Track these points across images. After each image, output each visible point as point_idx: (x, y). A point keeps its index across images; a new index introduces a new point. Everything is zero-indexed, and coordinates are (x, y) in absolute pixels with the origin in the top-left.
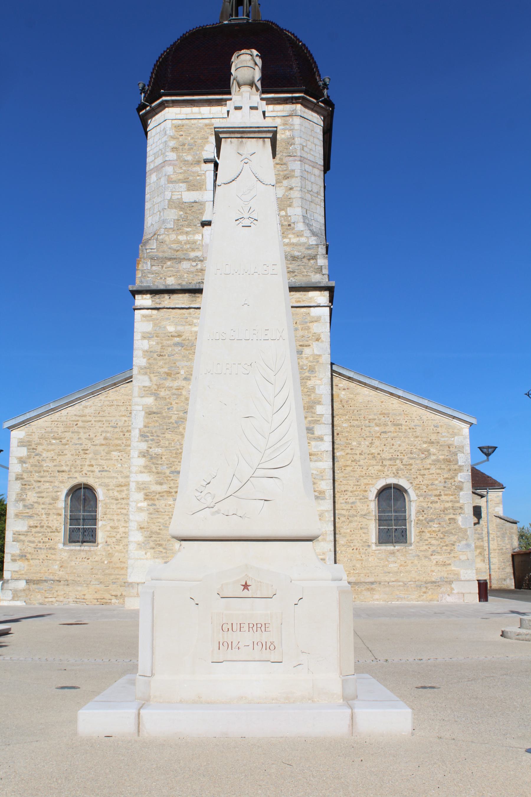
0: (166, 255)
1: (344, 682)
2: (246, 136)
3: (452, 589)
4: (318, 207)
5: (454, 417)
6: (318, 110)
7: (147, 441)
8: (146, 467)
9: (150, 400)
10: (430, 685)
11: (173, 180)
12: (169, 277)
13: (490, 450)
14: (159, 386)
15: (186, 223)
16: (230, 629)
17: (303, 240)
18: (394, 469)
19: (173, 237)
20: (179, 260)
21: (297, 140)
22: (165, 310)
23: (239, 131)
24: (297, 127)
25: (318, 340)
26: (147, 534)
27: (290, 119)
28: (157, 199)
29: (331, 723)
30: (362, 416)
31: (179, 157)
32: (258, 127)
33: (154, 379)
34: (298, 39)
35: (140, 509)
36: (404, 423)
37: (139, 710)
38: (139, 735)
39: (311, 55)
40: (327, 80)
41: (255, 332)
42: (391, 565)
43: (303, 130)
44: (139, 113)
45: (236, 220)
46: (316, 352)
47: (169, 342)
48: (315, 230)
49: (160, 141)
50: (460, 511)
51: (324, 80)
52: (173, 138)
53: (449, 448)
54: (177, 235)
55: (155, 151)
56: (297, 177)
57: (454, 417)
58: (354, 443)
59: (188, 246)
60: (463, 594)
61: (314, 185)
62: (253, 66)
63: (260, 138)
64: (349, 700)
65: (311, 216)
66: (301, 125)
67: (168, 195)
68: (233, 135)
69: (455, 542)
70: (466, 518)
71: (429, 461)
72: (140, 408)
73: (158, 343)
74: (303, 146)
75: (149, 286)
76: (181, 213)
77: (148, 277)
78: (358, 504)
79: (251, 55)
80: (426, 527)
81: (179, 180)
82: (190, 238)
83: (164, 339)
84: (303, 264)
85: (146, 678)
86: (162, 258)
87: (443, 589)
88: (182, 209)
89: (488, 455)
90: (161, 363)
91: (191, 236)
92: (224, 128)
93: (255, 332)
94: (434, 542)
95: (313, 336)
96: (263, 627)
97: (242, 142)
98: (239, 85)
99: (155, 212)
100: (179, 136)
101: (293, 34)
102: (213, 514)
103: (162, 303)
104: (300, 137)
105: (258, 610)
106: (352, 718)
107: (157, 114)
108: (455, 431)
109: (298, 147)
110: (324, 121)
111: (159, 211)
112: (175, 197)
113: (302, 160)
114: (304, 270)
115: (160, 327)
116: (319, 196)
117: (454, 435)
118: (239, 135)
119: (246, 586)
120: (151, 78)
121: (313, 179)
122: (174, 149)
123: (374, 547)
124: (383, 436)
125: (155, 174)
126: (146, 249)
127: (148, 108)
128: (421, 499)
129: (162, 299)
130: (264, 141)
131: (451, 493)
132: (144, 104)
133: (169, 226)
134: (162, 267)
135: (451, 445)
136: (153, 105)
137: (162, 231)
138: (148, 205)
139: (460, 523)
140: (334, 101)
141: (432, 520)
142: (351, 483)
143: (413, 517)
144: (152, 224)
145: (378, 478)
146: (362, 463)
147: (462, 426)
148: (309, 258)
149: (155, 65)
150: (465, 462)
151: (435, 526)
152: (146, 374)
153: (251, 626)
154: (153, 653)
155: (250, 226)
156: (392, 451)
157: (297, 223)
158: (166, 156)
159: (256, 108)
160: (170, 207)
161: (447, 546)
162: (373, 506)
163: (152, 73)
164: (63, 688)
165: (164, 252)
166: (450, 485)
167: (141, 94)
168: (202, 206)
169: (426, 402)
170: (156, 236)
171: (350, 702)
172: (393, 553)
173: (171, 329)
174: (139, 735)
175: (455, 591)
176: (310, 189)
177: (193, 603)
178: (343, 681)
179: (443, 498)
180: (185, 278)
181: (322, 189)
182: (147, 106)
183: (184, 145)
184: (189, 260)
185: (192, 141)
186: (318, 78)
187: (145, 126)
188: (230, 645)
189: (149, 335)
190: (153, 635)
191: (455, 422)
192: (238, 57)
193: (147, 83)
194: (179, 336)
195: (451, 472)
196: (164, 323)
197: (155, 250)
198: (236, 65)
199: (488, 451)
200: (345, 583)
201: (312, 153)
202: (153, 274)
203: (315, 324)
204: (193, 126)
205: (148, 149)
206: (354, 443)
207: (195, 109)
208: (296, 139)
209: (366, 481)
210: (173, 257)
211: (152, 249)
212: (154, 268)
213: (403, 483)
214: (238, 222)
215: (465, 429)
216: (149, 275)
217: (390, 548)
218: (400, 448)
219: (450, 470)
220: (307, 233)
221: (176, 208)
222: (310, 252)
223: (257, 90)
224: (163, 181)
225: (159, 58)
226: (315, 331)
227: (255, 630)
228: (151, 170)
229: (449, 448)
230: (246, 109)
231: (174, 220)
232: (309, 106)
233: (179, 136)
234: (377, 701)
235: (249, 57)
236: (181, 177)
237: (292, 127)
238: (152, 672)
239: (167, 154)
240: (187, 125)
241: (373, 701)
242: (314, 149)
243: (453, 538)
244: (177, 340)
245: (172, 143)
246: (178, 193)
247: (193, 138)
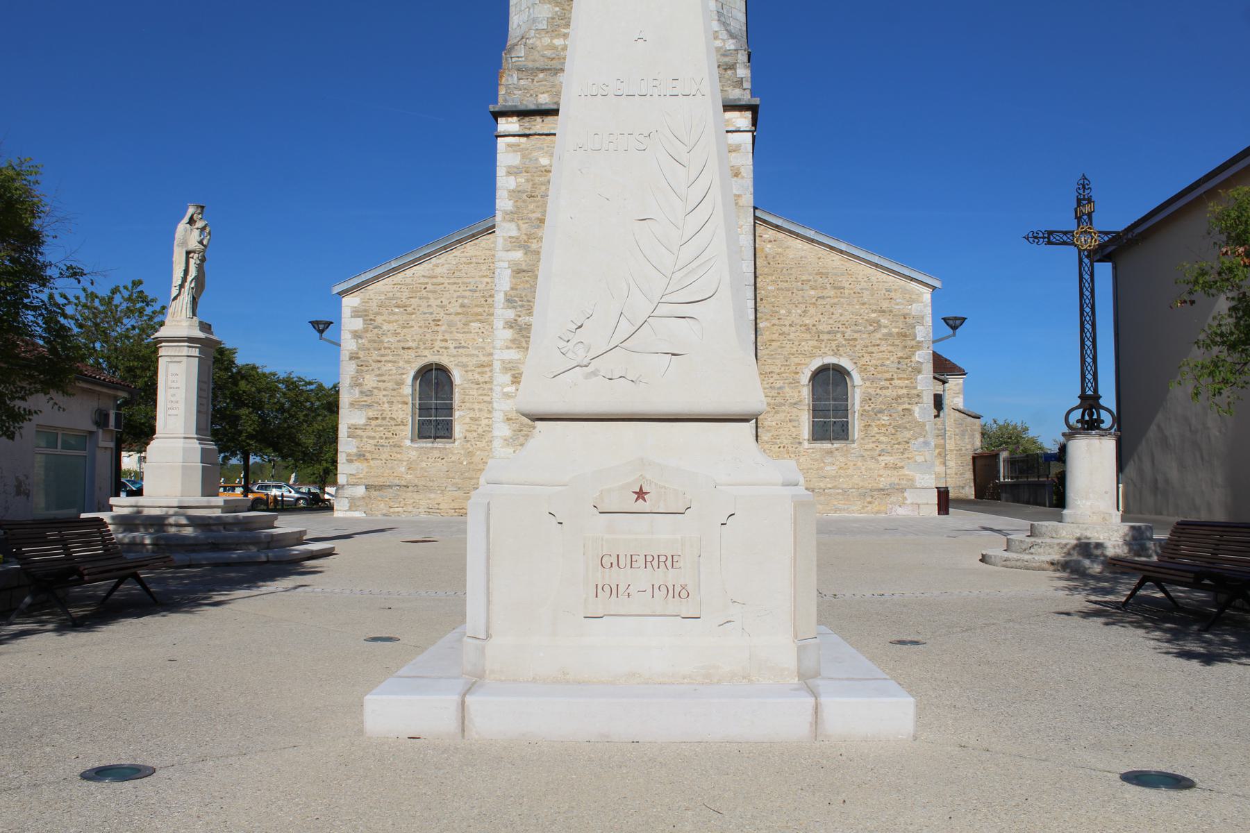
0: (537, 65)
1: (801, 649)
3: (905, 499)
5: (912, 279)
7: (514, 307)
8: (513, 341)
9: (518, 255)
10: (909, 638)
13: (958, 322)
14: (530, 236)
17: (718, 43)
18: (834, 344)
19: (546, 41)
25: (736, 175)
26: (516, 427)
29: (781, 719)
30: (793, 278)
33: (524, 227)
35: (507, 396)
36: (847, 285)
37: (464, 695)
38: (463, 737)
41: (655, 83)
42: (828, 468)
46: (735, 192)
50: (917, 400)
54: (552, 38)
58: (783, 312)
60: (919, 505)
64: (808, 680)
71: (878, 335)
72: (506, 264)
73: (527, 181)
78: (787, 389)
80: (873, 420)
87: (893, 499)
89: (954, 328)
90: (532, 207)
93: (655, 83)
94: (883, 439)
96: (669, 561)
102: (588, 376)
105: (660, 533)
106: (816, 713)
117: (911, 301)
123: (806, 445)
124: (821, 302)
128: (868, 384)
133: (540, 27)
137: (532, 33)
139: (916, 415)
141: (881, 411)
142: (778, 362)
143: (857, 407)
145: (812, 356)
146: (792, 336)
151: (885, 419)
152: (512, 220)
154: (489, 602)
156: (831, 321)
161: (899, 444)
162: (806, 392)
164: (375, 639)
165: (534, 61)
169: (876, 259)
171: (810, 681)
172: (830, 452)
174: (463, 737)
175: (908, 502)
177: (554, 521)
178: (799, 648)
179: (896, 382)
188: (615, 591)
190: (488, 574)
191: (913, 285)
200: (801, 490)
203: (733, 154)
206: (783, 312)
209: (797, 360)
212: (522, 82)
213: (845, 363)
215: (927, 294)
217: (827, 445)
218: (842, 318)
220: (724, 35)
222: (726, 59)
234: (852, 679)
238: (488, 628)
241: (847, 679)
243: (908, 434)
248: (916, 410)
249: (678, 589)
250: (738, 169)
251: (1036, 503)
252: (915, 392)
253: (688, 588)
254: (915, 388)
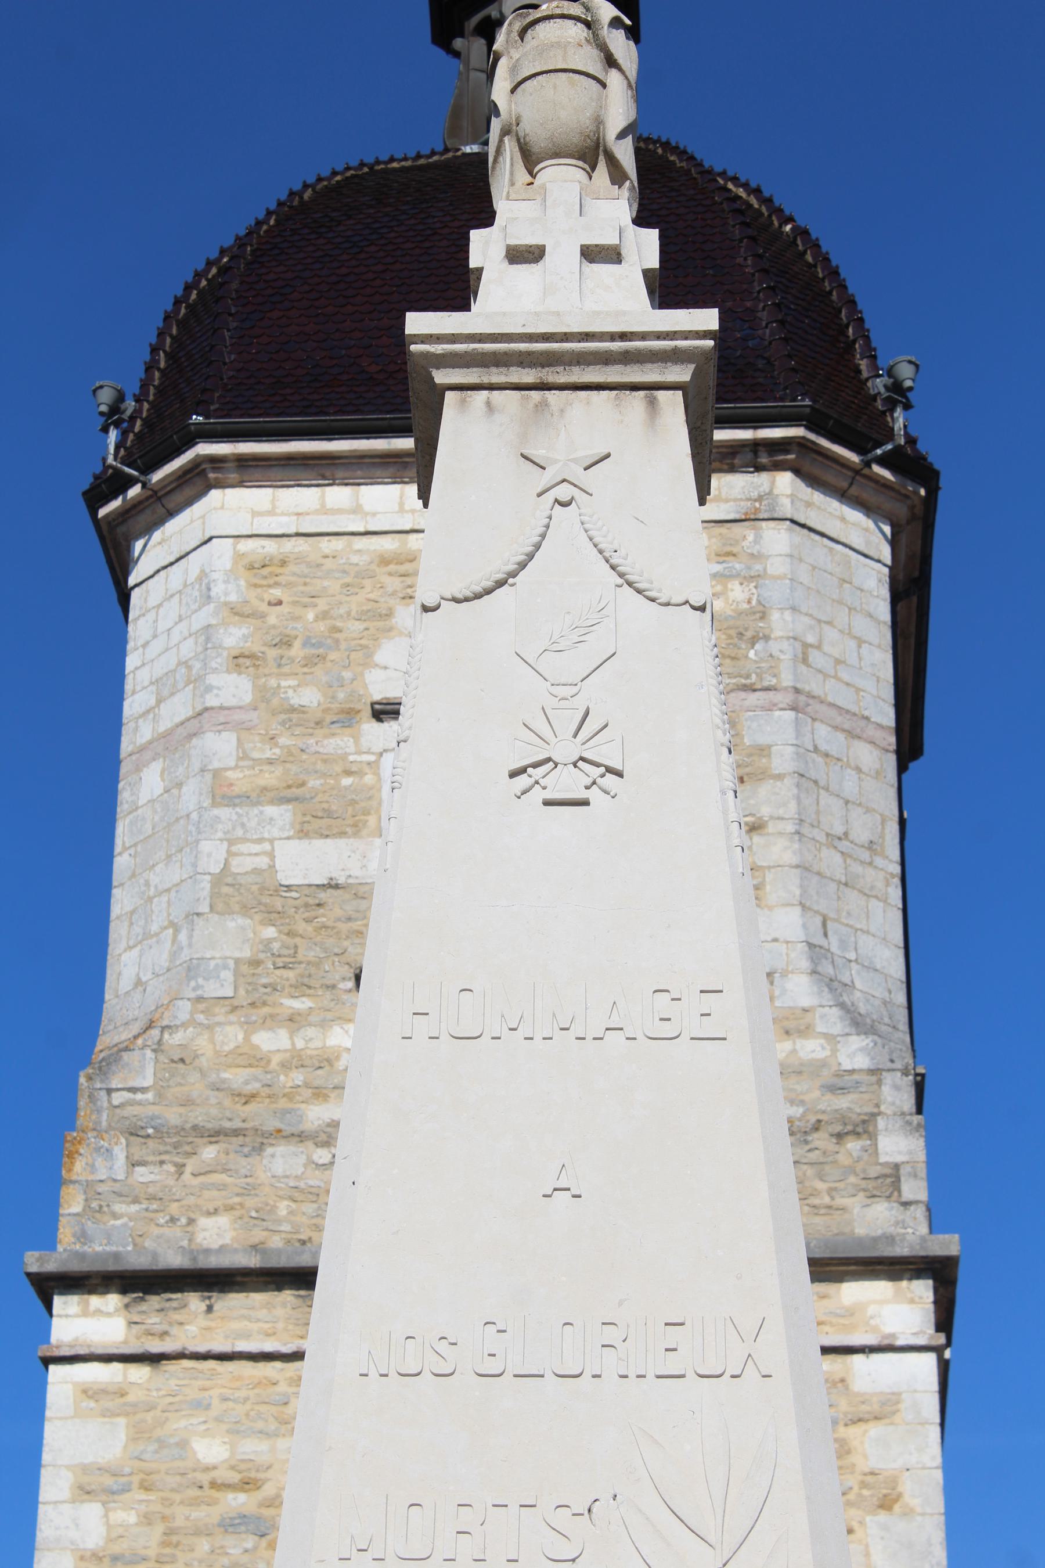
0: (197, 1116)
2: (562, 379)
4: (875, 905)
6: (868, 494)
11: (236, 790)
12: (209, 1214)
15: (290, 974)
17: (811, 1049)
19: (231, 1036)
20: (259, 1140)
21: (780, 622)
22: (186, 1363)
23: (529, 353)
24: (777, 567)
25: (887, 1503)
27: (747, 533)
28: (165, 875)
31: (263, 695)
32: (623, 336)
34: (779, 211)
39: (835, 273)
40: (905, 372)
41: (611, 1335)
43: (805, 577)
44: (93, 511)
45: (513, 774)
47: (199, 1514)
48: (862, 1009)
49: (183, 626)
51: (890, 373)
52: (238, 612)
54: (250, 1027)
55: (159, 670)
56: (780, 777)
59: (298, 1077)
61: (856, 813)
62: (595, 66)
63: (634, 387)
65: (843, 944)
66: (795, 557)
67: (212, 854)
68: (497, 376)
73: (147, 1519)
74: (806, 646)
75: (116, 1256)
76: (270, 932)
77: (115, 1216)
79: (588, 25)
81: (264, 789)
82: (309, 1040)
83: (178, 1497)
84: (813, 1156)
86: (180, 1130)
88: (272, 915)
91: (310, 1032)
93: (611, 1335)
95: (863, 1485)
97: (544, 404)
98: (531, 160)
99: (154, 928)
100: (264, 607)
101: (757, 191)
103: (175, 1330)
104: (794, 609)
107: (171, 514)
109: (783, 650)
110: (894, 543)
111: (172, 924)
112: (242, 865)
113: (801, 702)
114: (821, 1186)
115: (162, 1443)
116: (879, 861)
118: (529, 376)
120: (149, 368)
121: (850, 785)
122: (241, 660)
125: (157, 766)
126: (109, 1091)
127: (135, 491)
129: (177, 1317)
130: (652, 403)
132: (117, 472)
133: (212, 989)
134: (180, 1168)
136: (157, 476)
137: (183, 1010)
138: (121, 901)
140: (936, 460)
144: (139, 983)
148: (838, 1128)
149: (167, 318)
155: (585, 803)
157: (785, 974)
158: (209, 689)
159: (609, 255)
160: (220, 906)
163: (154, 350)
165: (188, 1102)
167: (105, 430)
168: (363, 904)
170: (155, 1033)
173: (211, 1450)
176: (839, 830)
180: (279, 1221)
181: (894, 828)
182: (131, 482)
183: (286, 642)
184: (301, 1137)
185: (322, 627)
186: (863, 364)
187: (120, 565)
189: (108, 1481)
192: (522, 33)
193: (133, 388)
194: (247, 1485)
196: (178, 1424)
197: (150, 1096)
198: (513, 69)
201: (844, 675)
202: (136, 1201)
203: (874, 1430)
204: (329, 564)
205: (131, 662)
207: (338, 495)
208: (775, 616)
210: (228, 1125)
211: (133, 1090)
212: (142, 1174)
214: (523, 781)
216: (119, 1208)
220: (831, 1021)
221: (245, 910)
222: (843, 1102)
223: (617, 176)
224: (192, 796)
225: (188, 288)
226: (873, 1463)
228: (142, 749)
230: (563, 256)
231: (237, 961)
232: (830, 478)
233: (264, 607)
235: (578, 31)
236: (271, 778)
237: (758, 567)
239: (212, 679)
240: (300, 559)
242: (853, 659)
244: (237, 1501)
245: (235, 637)
246: (256, 848)
247: (324, 616)
250: (893, 1482)
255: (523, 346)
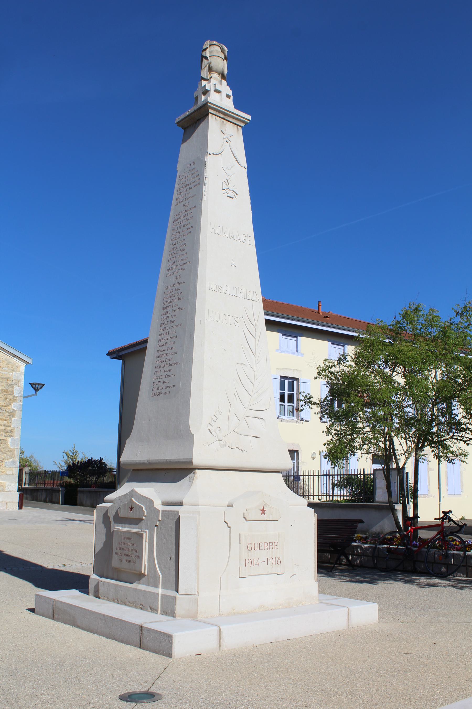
2: (227, 119)
5: (15, 356)
13: (40, 387)
16: (253, 548)
50: (10, 434)
53: (7, 380)
57: (15, 356)
60: (6, 503)
63: (235, 124)
68: (218, 114)
69: (4, 459)
70: (15, 440)
85: (190, 596)
89: (36, 390)
92: (214, 105)
96: (271, 545)
108: (14, 367)
117: (13, 370)
118: (222, 116)
119: (263, 511)
130: (238, 128)
131: (4, 418)
135: (9, 378)
139: (9, 444)
147: (20, 364)
150: (19, 394)
153: (266, 544)
155: (233, 198)
166: (4, 412)
195: (7, 401)
199: (37, 387)
215: (22, 367)
219: (6, 399)
227: (268, 548)
229: (7, 380)
248: (9, 440)
249: (277, 559)
251: (52, 502)
252: (9, 428)
253: (281, 559)
254: (10, 426)
255: (224, 111)
